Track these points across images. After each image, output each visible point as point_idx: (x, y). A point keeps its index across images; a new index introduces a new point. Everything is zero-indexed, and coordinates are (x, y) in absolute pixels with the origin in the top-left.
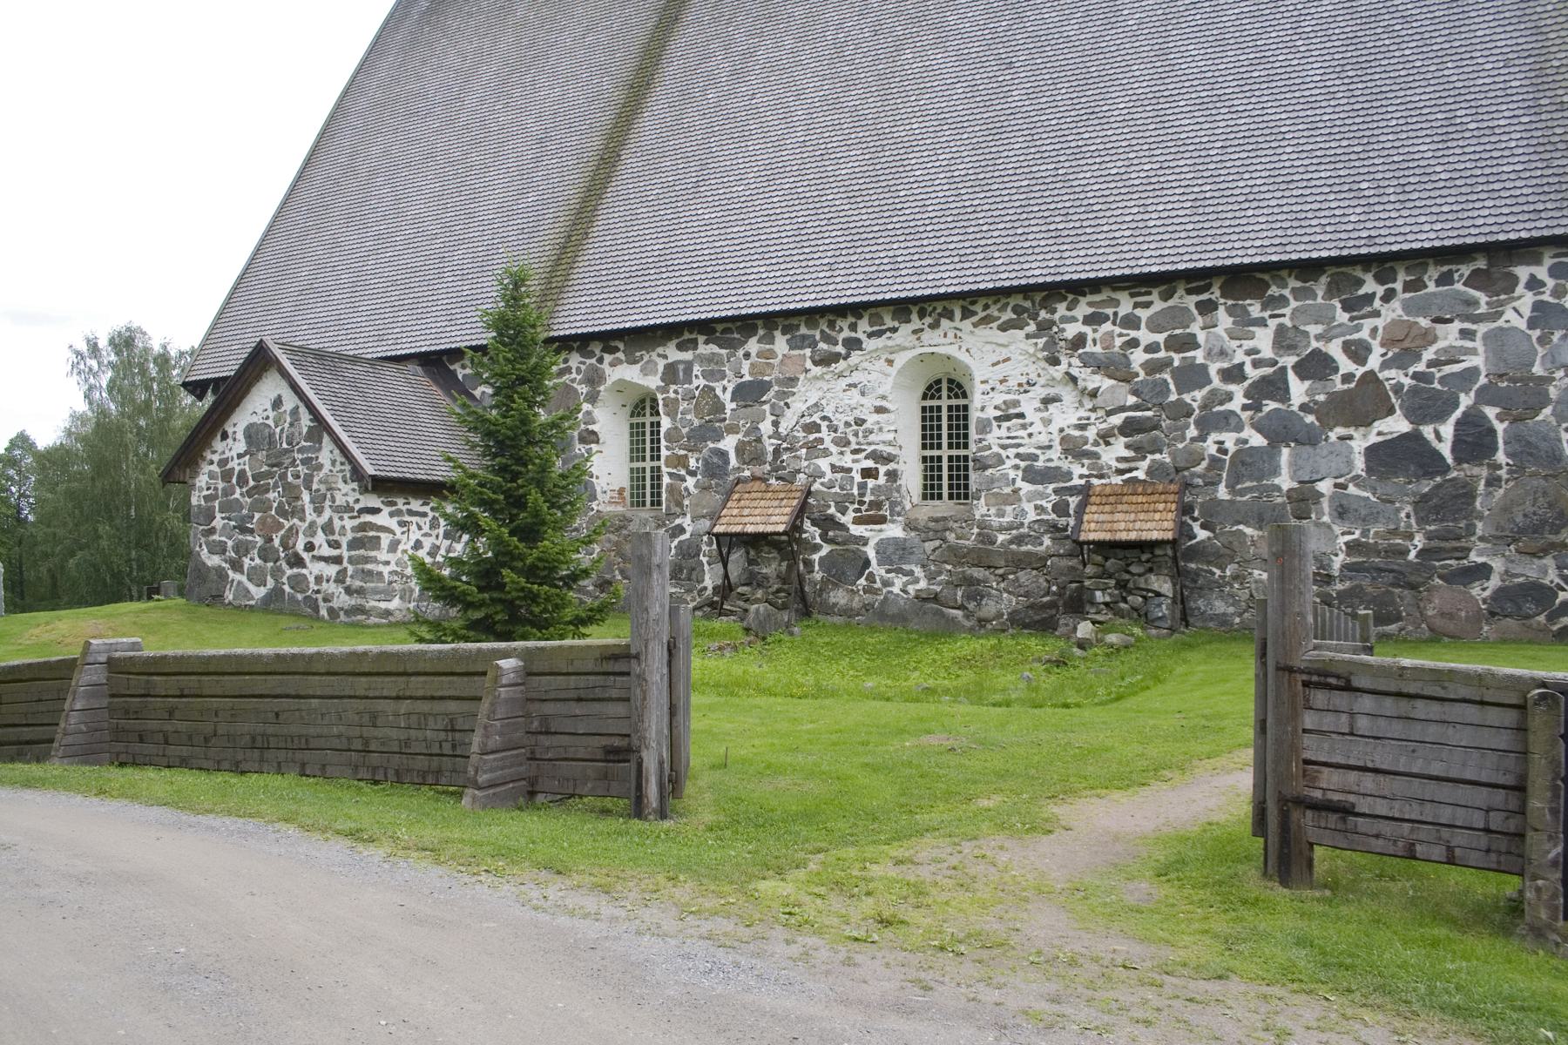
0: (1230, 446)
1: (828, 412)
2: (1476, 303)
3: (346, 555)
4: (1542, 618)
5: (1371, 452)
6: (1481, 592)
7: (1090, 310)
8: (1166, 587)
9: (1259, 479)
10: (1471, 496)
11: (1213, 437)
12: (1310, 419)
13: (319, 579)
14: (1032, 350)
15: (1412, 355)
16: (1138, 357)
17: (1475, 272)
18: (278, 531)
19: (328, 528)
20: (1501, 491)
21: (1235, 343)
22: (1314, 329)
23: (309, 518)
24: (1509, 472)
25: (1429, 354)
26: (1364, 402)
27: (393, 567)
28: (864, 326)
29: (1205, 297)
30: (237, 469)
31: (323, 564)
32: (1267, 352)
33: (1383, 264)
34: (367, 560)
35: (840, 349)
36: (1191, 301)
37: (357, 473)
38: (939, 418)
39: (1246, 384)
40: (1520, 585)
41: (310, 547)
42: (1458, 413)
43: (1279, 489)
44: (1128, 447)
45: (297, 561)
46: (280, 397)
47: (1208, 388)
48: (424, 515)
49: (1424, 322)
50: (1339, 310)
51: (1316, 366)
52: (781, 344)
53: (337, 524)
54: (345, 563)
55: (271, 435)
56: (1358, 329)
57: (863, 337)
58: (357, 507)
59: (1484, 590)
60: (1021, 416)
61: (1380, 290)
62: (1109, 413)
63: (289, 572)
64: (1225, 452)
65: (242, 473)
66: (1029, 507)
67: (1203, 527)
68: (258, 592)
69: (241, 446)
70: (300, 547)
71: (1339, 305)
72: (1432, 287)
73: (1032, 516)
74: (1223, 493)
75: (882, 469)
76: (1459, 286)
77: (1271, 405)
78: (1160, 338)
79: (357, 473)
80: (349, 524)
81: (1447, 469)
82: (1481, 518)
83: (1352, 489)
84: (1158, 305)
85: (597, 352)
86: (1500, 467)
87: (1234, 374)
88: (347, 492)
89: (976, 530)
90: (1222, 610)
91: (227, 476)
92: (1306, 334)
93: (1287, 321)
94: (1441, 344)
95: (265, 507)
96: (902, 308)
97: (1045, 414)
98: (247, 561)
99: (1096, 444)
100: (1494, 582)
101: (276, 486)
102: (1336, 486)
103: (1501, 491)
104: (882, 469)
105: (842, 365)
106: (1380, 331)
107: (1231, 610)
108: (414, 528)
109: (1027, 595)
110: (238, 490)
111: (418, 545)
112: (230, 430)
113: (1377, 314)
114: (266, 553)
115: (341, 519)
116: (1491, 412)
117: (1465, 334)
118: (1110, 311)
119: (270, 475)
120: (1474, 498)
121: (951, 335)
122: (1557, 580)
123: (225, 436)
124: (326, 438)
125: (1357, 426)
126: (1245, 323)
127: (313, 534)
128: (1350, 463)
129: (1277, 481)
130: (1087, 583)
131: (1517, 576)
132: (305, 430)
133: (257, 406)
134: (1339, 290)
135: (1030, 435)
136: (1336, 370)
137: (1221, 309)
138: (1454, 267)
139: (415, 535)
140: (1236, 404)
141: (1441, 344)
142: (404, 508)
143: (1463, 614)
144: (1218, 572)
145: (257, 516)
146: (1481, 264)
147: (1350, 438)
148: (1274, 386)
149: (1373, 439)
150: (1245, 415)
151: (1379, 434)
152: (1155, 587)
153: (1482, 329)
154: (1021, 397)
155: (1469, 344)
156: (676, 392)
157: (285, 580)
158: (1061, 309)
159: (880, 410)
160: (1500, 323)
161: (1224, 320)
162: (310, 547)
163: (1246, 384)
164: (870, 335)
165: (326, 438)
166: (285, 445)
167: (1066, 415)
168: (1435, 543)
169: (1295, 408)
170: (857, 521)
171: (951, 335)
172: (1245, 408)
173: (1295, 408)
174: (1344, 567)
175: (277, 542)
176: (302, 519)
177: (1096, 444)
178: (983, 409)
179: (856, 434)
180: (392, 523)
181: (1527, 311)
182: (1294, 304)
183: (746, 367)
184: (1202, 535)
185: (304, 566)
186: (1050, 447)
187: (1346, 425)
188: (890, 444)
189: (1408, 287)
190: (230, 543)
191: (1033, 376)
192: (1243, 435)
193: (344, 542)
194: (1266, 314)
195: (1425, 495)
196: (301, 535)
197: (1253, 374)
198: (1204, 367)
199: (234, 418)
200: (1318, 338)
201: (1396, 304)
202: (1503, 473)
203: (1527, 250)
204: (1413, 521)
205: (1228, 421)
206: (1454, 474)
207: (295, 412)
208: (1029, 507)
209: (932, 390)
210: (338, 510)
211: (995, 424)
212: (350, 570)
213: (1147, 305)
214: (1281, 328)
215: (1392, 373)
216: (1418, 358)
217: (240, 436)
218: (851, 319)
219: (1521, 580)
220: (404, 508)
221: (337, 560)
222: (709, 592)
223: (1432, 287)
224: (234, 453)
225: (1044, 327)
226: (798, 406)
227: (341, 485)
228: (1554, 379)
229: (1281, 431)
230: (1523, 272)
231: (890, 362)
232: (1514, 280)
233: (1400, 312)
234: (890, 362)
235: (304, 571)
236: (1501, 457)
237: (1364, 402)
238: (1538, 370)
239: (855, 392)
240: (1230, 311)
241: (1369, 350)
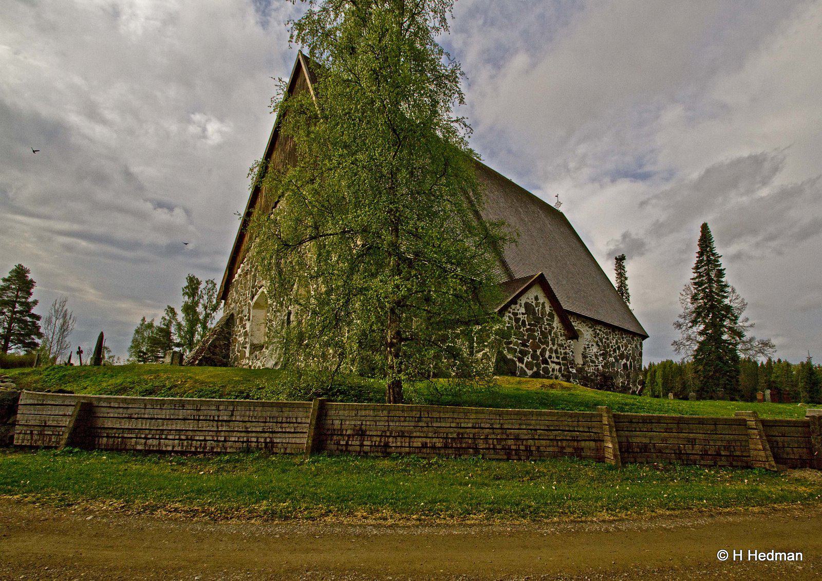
13: (553, 370)
19: (556, 352)
30: (522, 319)
41: (550, 357)
45: (545, 362)
53: (559, 350)
55: (534, 310)
63: (542, 366)
65: (524, 322)
70: (547, 356)
91: (517, 320)
95: (534, 338)
98: (526, 359)
114: (534, 357)
115: (560, 349)
119: (536, 326)
127: (552, 354)
132: (548, 313)
145: (531, 341)
162: (550, 357)
175: (538, 353)
176: (548, 346)
185: (549, 365)
193: (561, 357)
207: (543, 304)
210: (559, 345)
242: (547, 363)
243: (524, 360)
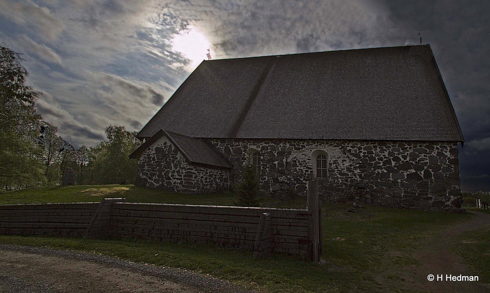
1: (298, 158)
3: (183, 178)
6: (431, 202)
7: (352, 145)
8: (369, 197)
12: (396, 168)
14: (340, 151)
16: (362, 154)
18: (163, 172)
21: (380, 154)
23: (173, 169)
25: (418, 159)
26: (407, 166)
27: (195, 181)
28: (306, 143)
30: (152, 157)
31: (176, 180)
32: (387, 156)
33: (409, 142)
34: (189, 180)
35: (300, 147)
36: (372, 145)
37: (187, 160)
38: (320, 162)
44: (360, 170)
46: (166, 142)
47: (375, 161)
48: (204, 171)
51: (397, 159)
52: (288, 145)
54: (183, 180)
56: (405, 153)
57: (305, 145)
58: (187, 168)
60: (338, 163)
61: (409, 147)
62: (356, 164)
63: (166, 181)
66: (340, 180)
67: (375, 186)
68: (156, 185)
69: (154, 152)
73: (341, 181)
74: (379, 180)
75: (309, 171)
78: (366, 151)
79: (187, 160)
80: (184, 171)
83: (404, 181)
84: (365, 146)
85: (246, 142)
87: (381, 159)
88: (184, 164)
89: (329, 183)
90: (380, 202)
92: (395, 153)
96: (314, 141)
97: (343, 163)
98: (154, 178)
99: (353, 169)
100: (433, 200)
101: (164, 161)
102: (401, 181)
104: (309, 171)
105: (301, 150)
107: (382, 202)
108: (201, 173)
109: (340, 196)
110: (152, 162)
111: (202, 177)
112: (151, 148)
113: (408, 151)
114: (160, 176)
116: (430, 170)
118: (356, 146)
121: (324, 147)
123: (149, 149)
124: (179, 152)
126: (382, 151)
130: (354, 195)
133: (160, 143)
135: (340, 167)
137: (378, 148)
139: (201, 175)
141: (420, 157)
142: (199, 169)
145: (158, 168)
147: (404, 172)
150: (383, 167)
152: (367, 197)
153: (428, 155)
154: (338, 160)
156: (264, 152)
157: (165, 182)
158: (346, 144)
159: (309, 159)
160: (431, 155)
162: (172, 176)
164: (307, 145)
165: (179, 152)
166: (167, 153)
167: (347, 164)
169: (393, 166)
170: (304, 180)
171: (324, 147)
172: (383, 165)
173: (393, 166)
177: (353, 169)
178: (330, 161)
179: (304, 163)
180: (196, 172)
181: (436, 153)
183: (280, 148)
184: (375, 188)
185: (171, 180)
186: (344, 169)
188: (311, 166)
190: (149, 173)
191: (340, 156)
192: (383, 170)
196: (170, 173)
199: (152, 145)
200: (397, 154)
203: (436, 142)
205: (380, 168)
207: (170, 146)
208: (340, 180)
209: (319, 157)
211: (333, 164)
212: (184, 181)
213: (363, 145)
214: (389, 151)
217: (154, 149)
218: (303, 142)
220: (199, 169)
221: (181, 179)
222: (271, 191)
224: (152, 153)
225: (343, 147)
226: (291, 157)
227: (183, 163)
229: (390, 170)
230: (435, 146)
231: (311, 151)
234: (311, 151)
235: (171, 181)
237: (407, 166)
239: (304, 155)
240: (379, 148)
242: (170, 179)
243: (153, 178)
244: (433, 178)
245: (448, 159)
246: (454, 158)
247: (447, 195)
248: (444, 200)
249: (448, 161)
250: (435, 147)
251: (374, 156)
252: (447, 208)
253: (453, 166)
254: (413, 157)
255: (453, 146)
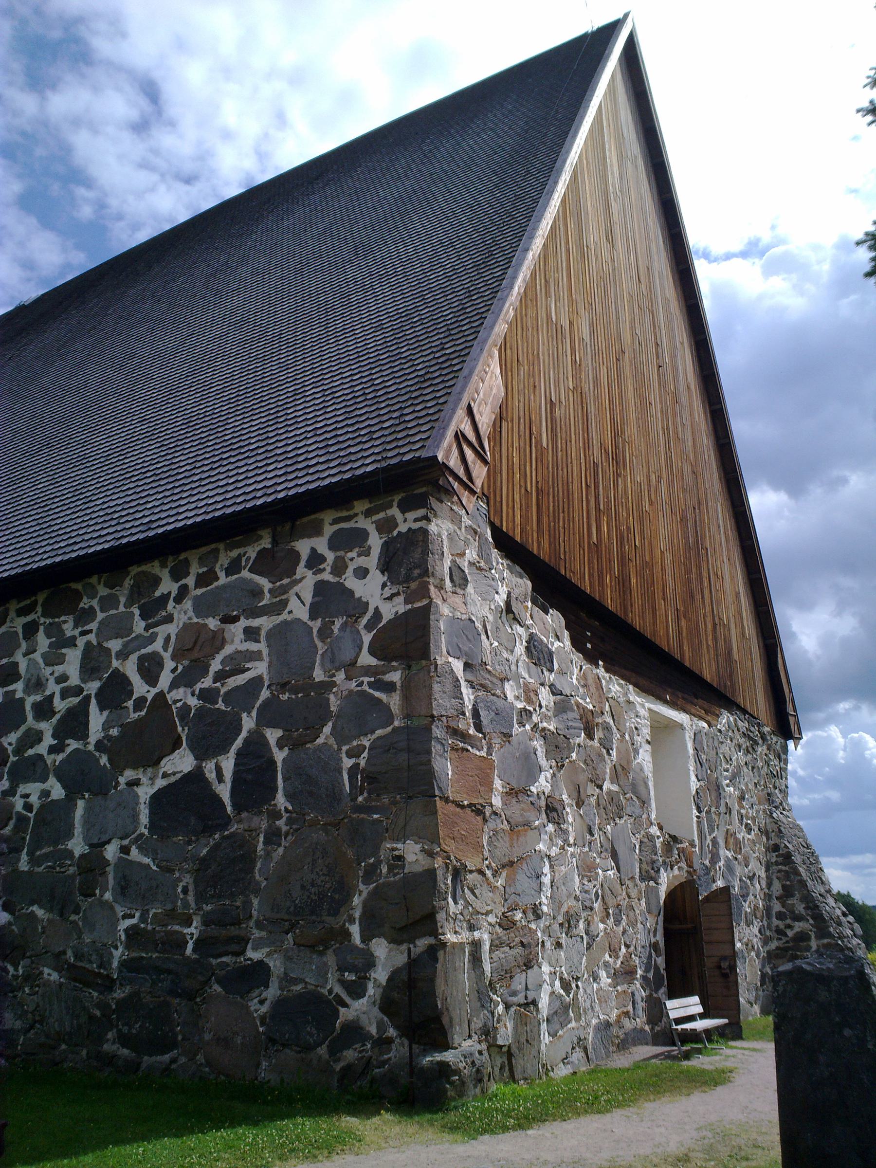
0: (34, 799)
2: (257, 593)
4: (323, 1051)
5: (156, 799)
6: (261, 1004)
9: (56, 843)
10: (248, 859)
11: (22, 789)
15: (198, 669)
17: (262, 553)
20: (281, 850)
21: (49, 670)
22: (115, 645)
24: (289, 822)
25: (216, 665)
26: (145, 741)
29: (29, 618)
32: (74, 680)
39: (54, 720)
40: (300, 995)
42: (239, 742)
43: (70, 853)
47: (23, 729)
49: (213, 623)
50: (137, 617)
56: (152, 639)
59: (261, 1002)
64: (28, 807)
71: (137, 612)
72: (223, 579)
76: (245, 574)
77: (73, 745)
81: (226, 821)
82: (257, 891)
83: (135, 854)
86: (277, 815)
93: (92, 637)
94: (228, 650)
100: (272, 992)
103: (281, 850)
106: (173, 638)
113: (169, 619)
116: (273, 735)
117: (251, 634)
120: (253, 862)
122: (338, 990)
125: (145, 766)
128: (135, 817)
129: (70, 845)
131: (296, 981)
134: (140, 594)
136: (131, 692)
138: (241, 551)
140: (42, 749)
141: (228, 650)
143: (239, 1040)
144: (11, 969)
146: (266, 543)
148: (74, 724)
149: (160, 783)
150: (49, 759)
151: (165, 775)
153: (265, 623)
155: (253, 647)
160: (284, 616)
161: (43, 642)
163: (54, 720)
168: (214, 931)
169: (91, 748)
172: (52, 750)
174: (123, 964)
181: (308, 597)
182: (100, 616)
187: (135, 767)
189: (203, 580)
192: (46, 786)
194: (76, 632)
195: (203, 860)
197: (60, 705)
198: (22, 701)
201: (188, 604)
202: (281, 823)
204: (191, 898)
206: (234, 828)
214: (88, 644)
215: (179, 693)
216: (205, 671)
219: (299, 988)
223: (223, 579)
228: (334, 684)
229: (81, 778)
230: (303, 547)
232: (297, 556)
233: (191, 613)
236: (281, 801)
238: (319, 675)
241: (161, 665)
244: (281, 801)
245: (369, 627)
246: (402, 609)
247: (355, 930)
248: (333, 985)
249: (367, 638)
250: (304, 556)
251: (19, 694)
252: (350, 1055)
253: (395, 677)
254: (195, 650)
255: (399, 517)
